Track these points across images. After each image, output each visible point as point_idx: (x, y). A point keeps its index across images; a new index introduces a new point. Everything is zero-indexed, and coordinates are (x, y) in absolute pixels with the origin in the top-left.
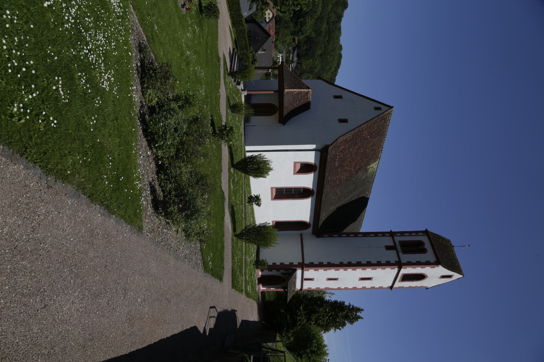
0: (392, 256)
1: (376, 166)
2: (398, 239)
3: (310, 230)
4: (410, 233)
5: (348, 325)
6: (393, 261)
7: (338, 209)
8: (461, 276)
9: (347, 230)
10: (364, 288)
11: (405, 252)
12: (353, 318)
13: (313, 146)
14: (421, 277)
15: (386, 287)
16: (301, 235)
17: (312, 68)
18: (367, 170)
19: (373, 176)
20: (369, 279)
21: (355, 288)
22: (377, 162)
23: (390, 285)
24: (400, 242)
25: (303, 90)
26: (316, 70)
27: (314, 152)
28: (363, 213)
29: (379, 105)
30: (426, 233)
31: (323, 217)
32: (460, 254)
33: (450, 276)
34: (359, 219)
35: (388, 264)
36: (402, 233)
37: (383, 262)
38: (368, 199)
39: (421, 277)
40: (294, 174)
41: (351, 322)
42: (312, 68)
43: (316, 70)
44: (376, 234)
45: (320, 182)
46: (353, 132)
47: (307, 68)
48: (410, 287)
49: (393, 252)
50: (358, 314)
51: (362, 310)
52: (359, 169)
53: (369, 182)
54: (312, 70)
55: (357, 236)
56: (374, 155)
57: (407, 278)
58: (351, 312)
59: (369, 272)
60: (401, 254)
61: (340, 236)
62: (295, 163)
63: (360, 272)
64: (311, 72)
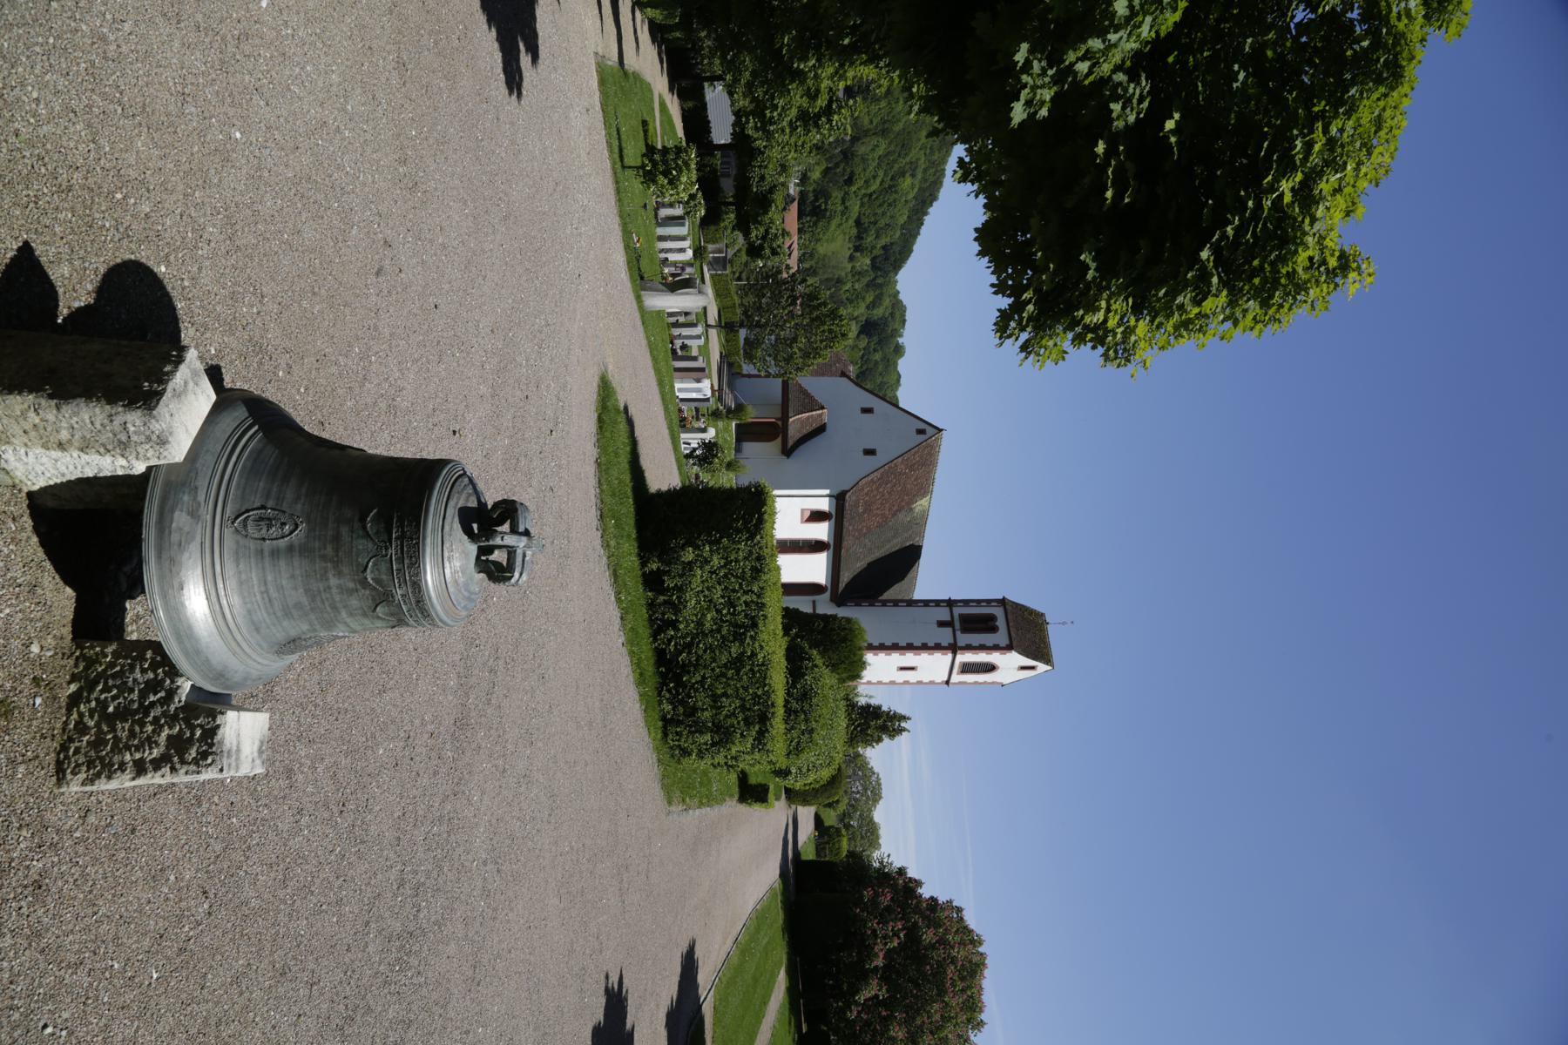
0: (945, 636)
1: (927, 504)
2: (957, 611)
3: (827, 595)
4: (978, 602)
5: (886, 740)
6: (945, 644)
7: (869, 564)
8: (1049, 668)
9: (889, 594)
10: (906, 683)
11: (965, 630)
12: (894, 730)
13: (827, 492)
14: (990, 668)
15: (940, 681)
16: (814, 602)
17: (885, 122)
18: (911, 509)
19: (924, 516)
20: (912, 669)
21: (893, 683)
22: (928, 497)
23: (945, 679)
24: (962, 616)
25: (814, 413)
26: (898, 127)
27: (827, 499)
28: (915, 567)
29: (923, 426)
30: (1003, 602)
31: (846, 577)
32: (1055, 635)
33: (1032, 668)
34: (910, 575)
35: (938, 647)
36: (966, 603)
37: (931, 644)
38: (920, 548)
39: (990, 668)
40: (802, 522)
41: (892, 737)
42: (885, 122)
43: (898, 127)
44: (926, 603)
45: (838, 532)
46: (882, 470)
47: (871, 122)
48: (976, 683)
49: (949, 630)
50: (903, 724)
51: (909, 719)
52: (899, 510)
53: (920, 523)
54: (886, 126)
55: (897, 606)
56: (924, 488)
57: (968, 668)
58: (891, 721)
59: (909, 658)
60: (958, 633)
61: (872, 605)
62: (803, 510)
63: (897, 659)
64: (884, 132)
